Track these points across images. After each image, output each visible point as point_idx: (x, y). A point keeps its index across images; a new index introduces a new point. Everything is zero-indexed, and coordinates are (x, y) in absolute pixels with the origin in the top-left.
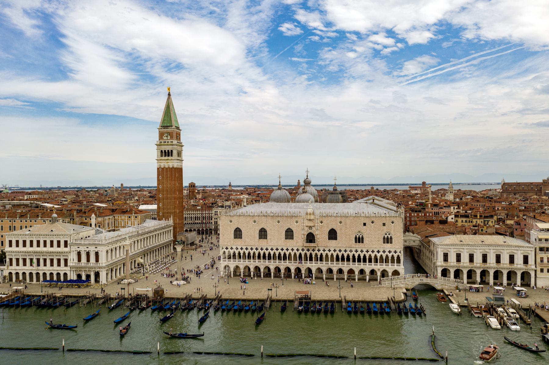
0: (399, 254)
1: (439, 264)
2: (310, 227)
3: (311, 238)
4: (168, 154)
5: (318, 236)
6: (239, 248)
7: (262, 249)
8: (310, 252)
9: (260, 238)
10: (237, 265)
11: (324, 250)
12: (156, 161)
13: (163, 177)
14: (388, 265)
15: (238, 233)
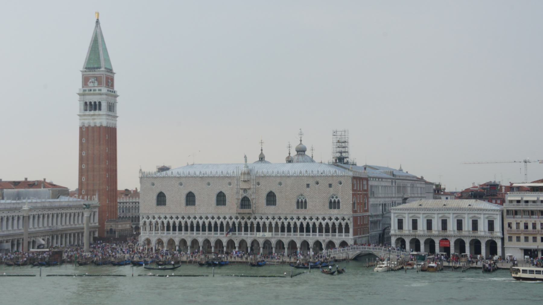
0: (349, 222)
1: (392, 232)
2: (245, 190)
3: (245, 203)
4: (95, 106)
5: (254, 201)
6: (162, 216)
7: (189, 218)
8: (245, 220)
9: (187, 204)
10: (160, 237)
11: (261, 218)
12: (78, 117)
13: (87, 140)
14: (335, 235)
15: (161, 199)
